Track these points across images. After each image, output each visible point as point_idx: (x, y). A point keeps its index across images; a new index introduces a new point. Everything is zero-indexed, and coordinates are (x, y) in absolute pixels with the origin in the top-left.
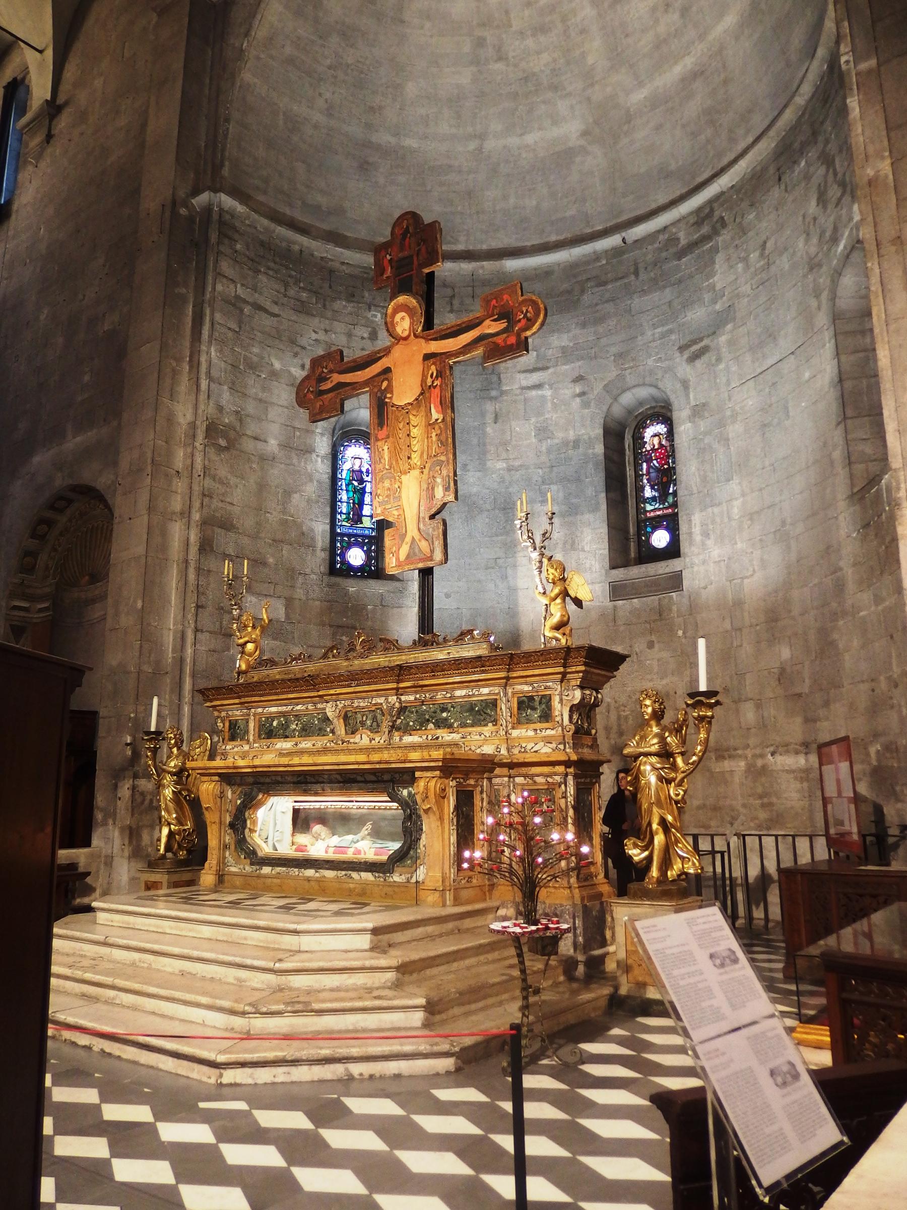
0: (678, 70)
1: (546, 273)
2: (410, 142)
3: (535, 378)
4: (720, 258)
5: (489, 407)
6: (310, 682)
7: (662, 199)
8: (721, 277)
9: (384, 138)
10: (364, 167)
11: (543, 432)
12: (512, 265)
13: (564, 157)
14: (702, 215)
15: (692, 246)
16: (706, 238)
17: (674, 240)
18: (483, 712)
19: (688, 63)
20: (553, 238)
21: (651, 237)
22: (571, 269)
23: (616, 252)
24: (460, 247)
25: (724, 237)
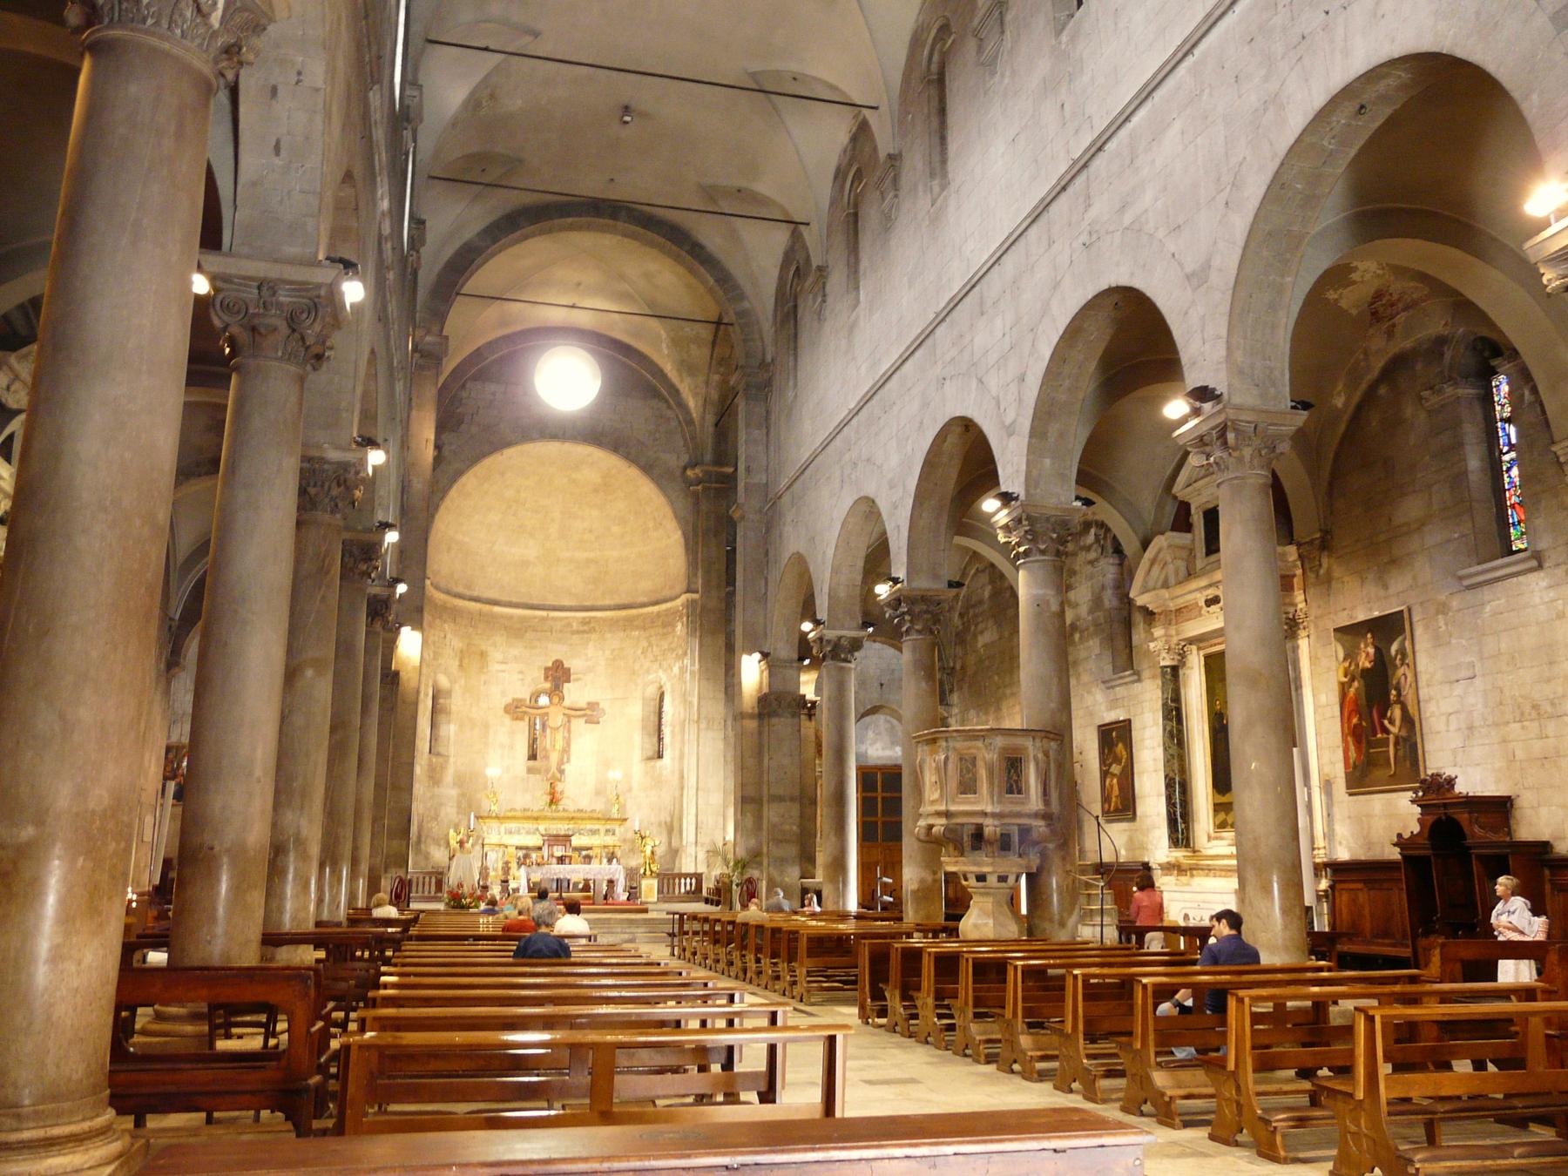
0: (586, 555)
1: (511, 617)
2: (467, 539)
3: (503, 667)
4: (591, 644)
5: (483, 678)
6: (536, 819)
7: (566, 602)
8: (590, 651)
9: (459, 537)
10: (449, 550)
11: (503, 693)
12: (497, 609)
13: (525, 564)
14: (585, 622)
15: (578, 632)
16: (584, 632)
17: (569, 625)
18: (594, 832)
19: (592, 555)
20: (514, 600)
21: (561, 619)
22: (523, 619)
23: (543, 619)
24: (475, 594)
25: (593, 636)
